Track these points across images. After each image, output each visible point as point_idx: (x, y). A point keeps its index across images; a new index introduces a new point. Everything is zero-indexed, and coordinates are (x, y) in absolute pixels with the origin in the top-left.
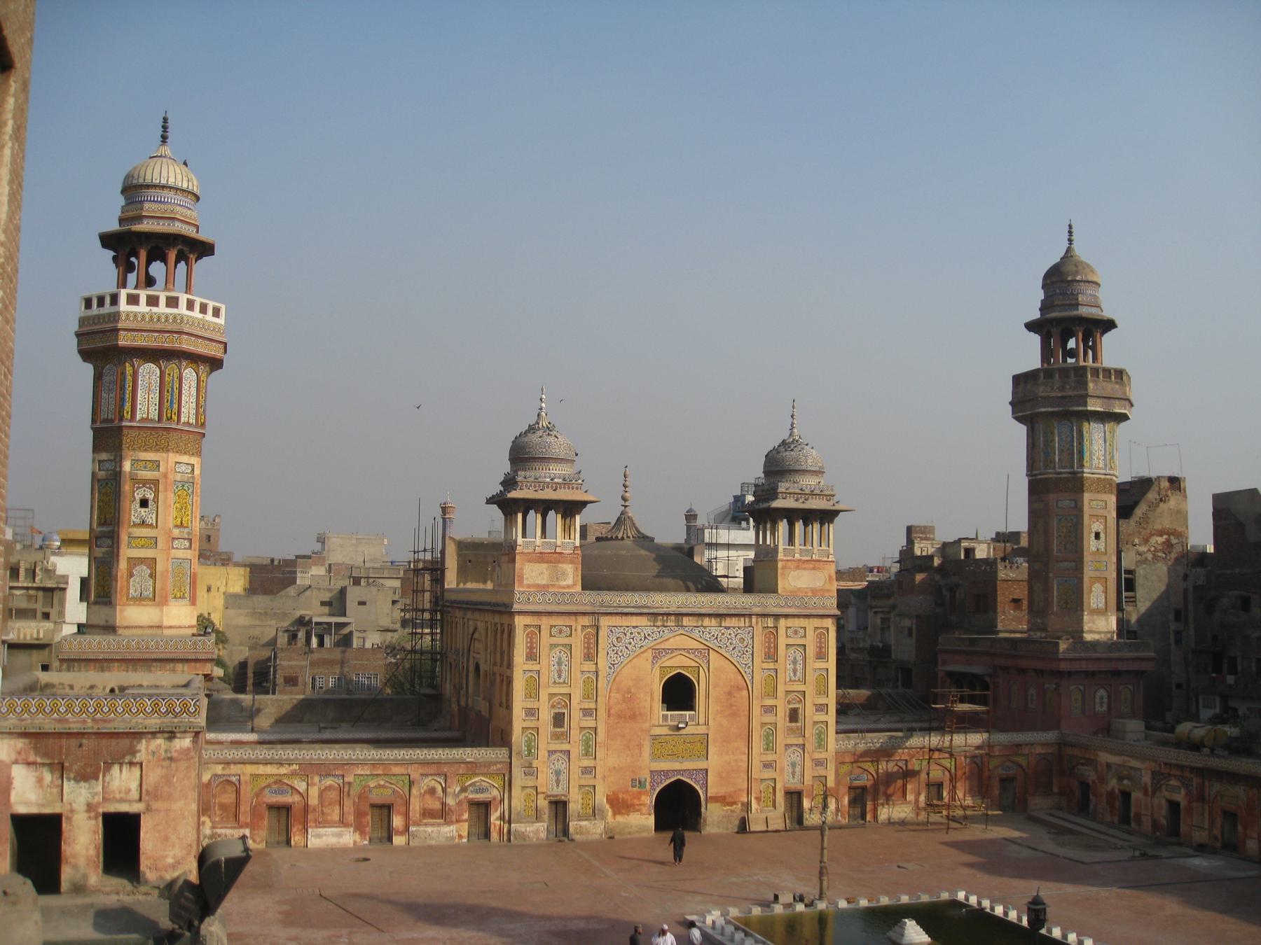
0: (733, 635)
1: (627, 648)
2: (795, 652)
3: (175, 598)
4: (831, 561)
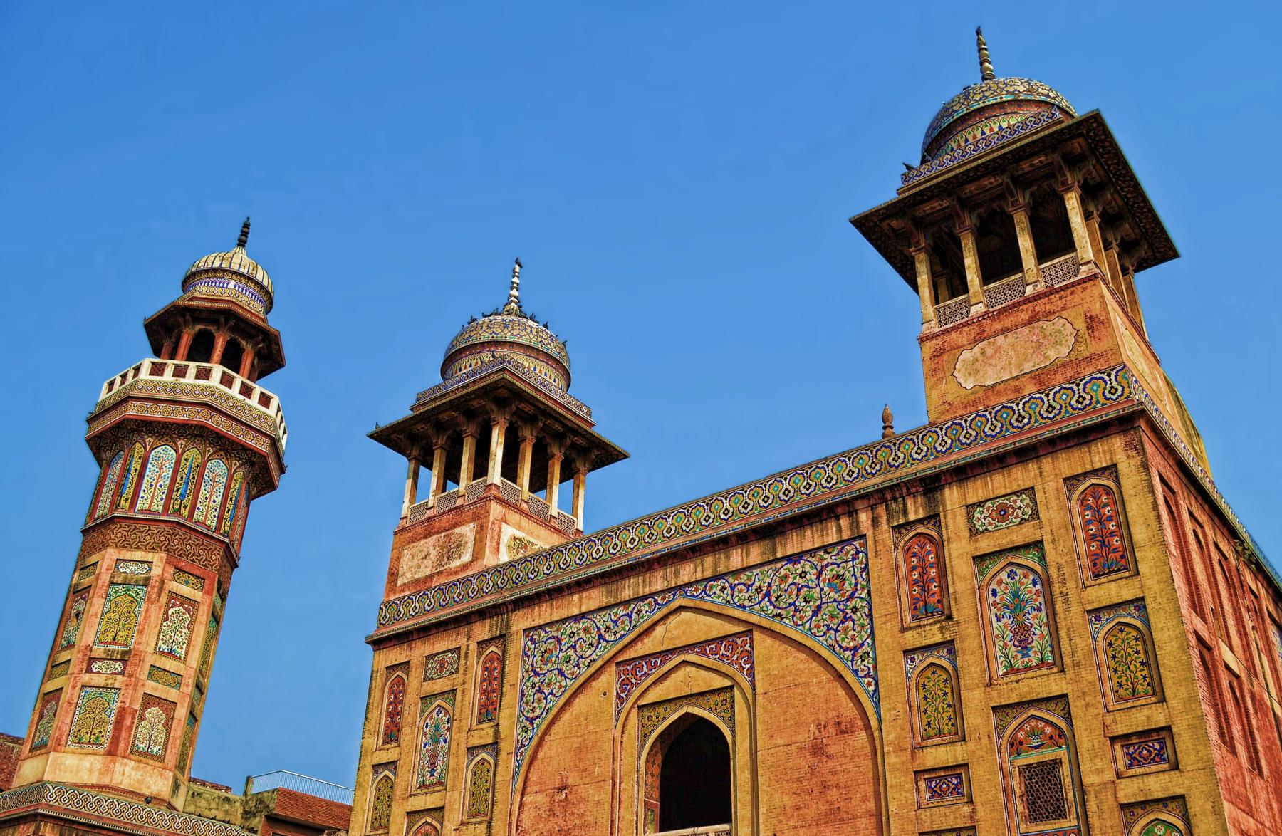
0: (812, 575)
1: (561, 673)
2: (1012, 575)
3: (78, 743)
4: (1084, 281)
